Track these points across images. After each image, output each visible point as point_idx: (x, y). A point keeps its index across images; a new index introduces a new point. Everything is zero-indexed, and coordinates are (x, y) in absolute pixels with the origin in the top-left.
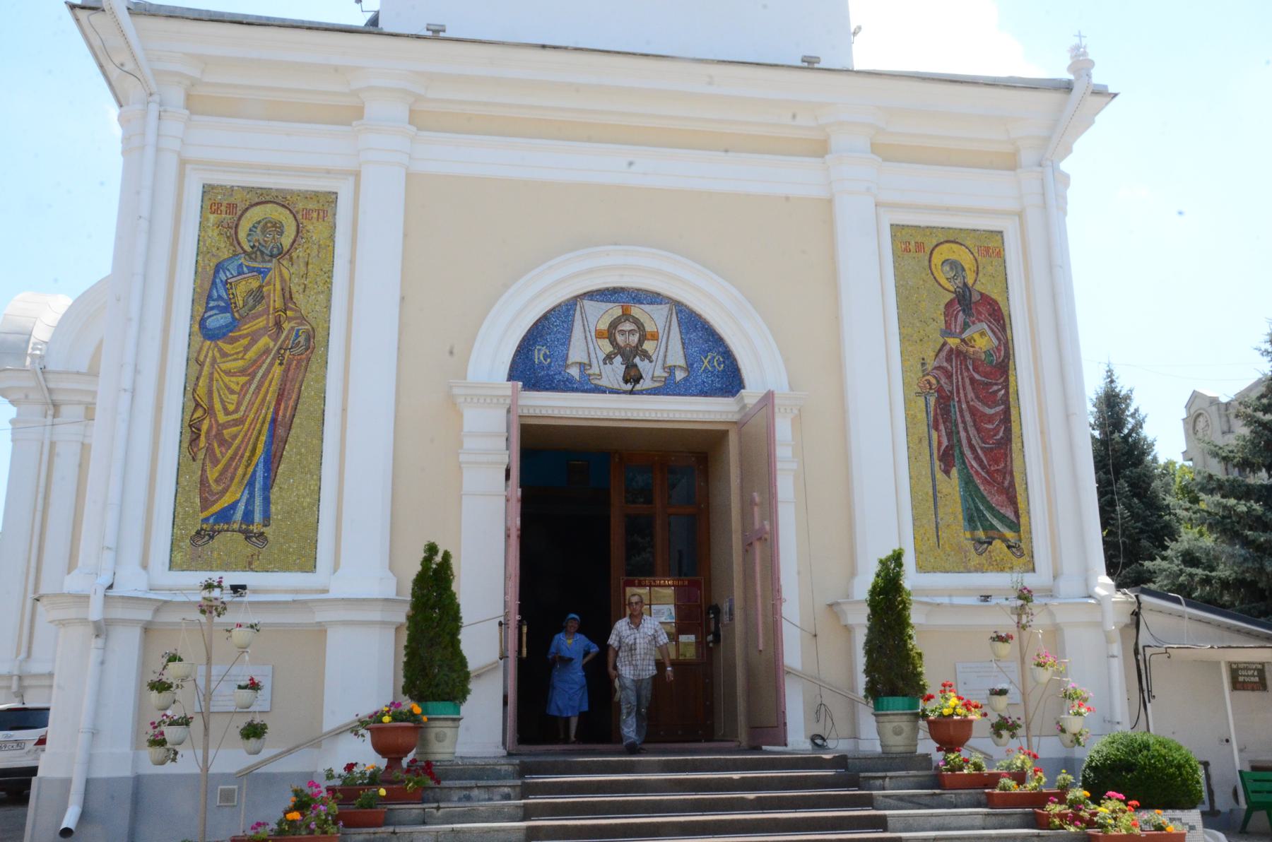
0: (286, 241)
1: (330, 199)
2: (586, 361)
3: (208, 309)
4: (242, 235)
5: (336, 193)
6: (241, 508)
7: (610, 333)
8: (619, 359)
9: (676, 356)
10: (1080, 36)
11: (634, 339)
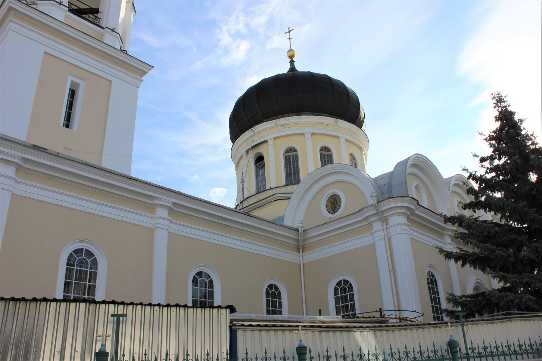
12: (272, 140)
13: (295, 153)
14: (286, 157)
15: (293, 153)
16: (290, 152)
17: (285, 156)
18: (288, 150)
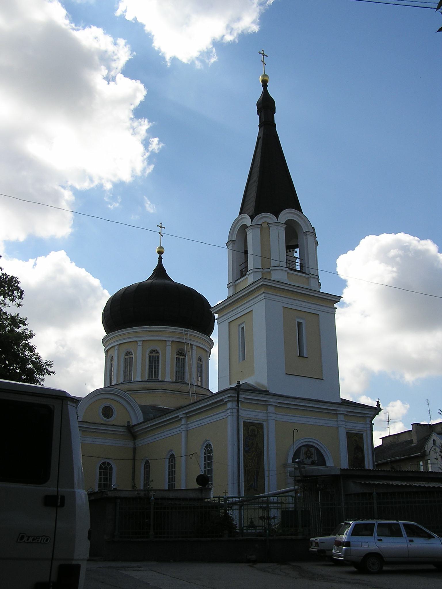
0: (256, 433)
1: (262, 425)
2: (303, 458)
3: (245, 446)
4: (249, 432)
5: (263, 424)
6: (253, 484)
7: (306, 453)
8: (307, 458)
9: (316, 459)
10: (379, 399)
11: (310, 455)
12: (141, 342)
13: (157, 354)
14: (150, 356)
15: (156, 354)
16: (153, 353)
17: (150, 356)
18: (152, 351)
